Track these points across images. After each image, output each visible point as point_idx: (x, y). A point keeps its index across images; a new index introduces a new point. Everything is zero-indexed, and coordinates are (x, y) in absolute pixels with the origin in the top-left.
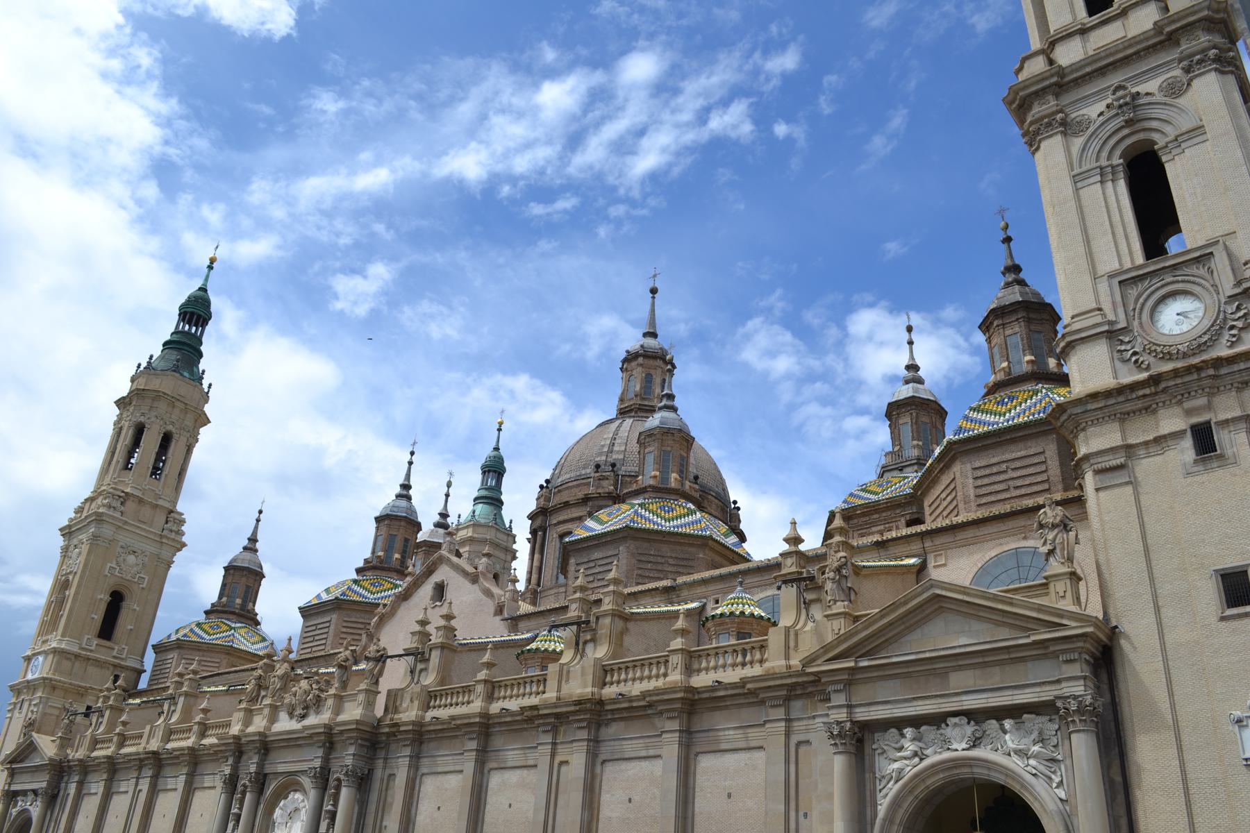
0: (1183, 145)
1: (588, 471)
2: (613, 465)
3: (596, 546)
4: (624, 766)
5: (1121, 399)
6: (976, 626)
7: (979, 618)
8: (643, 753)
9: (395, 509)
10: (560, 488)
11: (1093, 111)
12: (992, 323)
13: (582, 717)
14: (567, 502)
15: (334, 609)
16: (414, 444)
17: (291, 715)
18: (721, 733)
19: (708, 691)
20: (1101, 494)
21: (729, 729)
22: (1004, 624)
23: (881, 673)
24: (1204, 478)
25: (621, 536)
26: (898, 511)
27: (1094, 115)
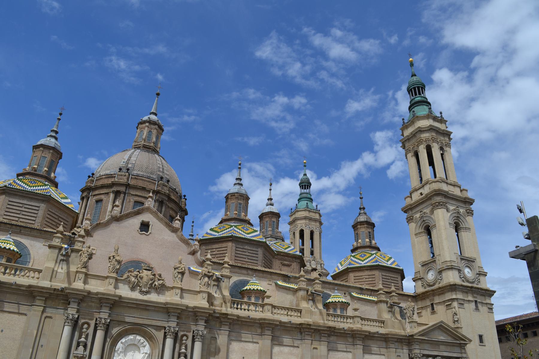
0: (467, 230)
1: (154, 177)
2: (168, 181)
3: (247, 243)
4: (336, 353)
5: (465, 288)
6: (445, 335)
7: (446, 333)
8: (345, 350)
9: (56, 146)
10: (137, 177)
11: (451, 208)
12: (364, 224)
13: (326, 332)
14: (145, 188)
15: (43, 201)
16: (63, 109)
17: (133, 289)
18: (372, 348)
19: (372, 334)
20: (460, 309)
21: (375, 347)
22: (450, 336)
23: (427, 342)
24: (476, 313)
25: (261, 244)
26: (294, 259)
27: (451, 209)
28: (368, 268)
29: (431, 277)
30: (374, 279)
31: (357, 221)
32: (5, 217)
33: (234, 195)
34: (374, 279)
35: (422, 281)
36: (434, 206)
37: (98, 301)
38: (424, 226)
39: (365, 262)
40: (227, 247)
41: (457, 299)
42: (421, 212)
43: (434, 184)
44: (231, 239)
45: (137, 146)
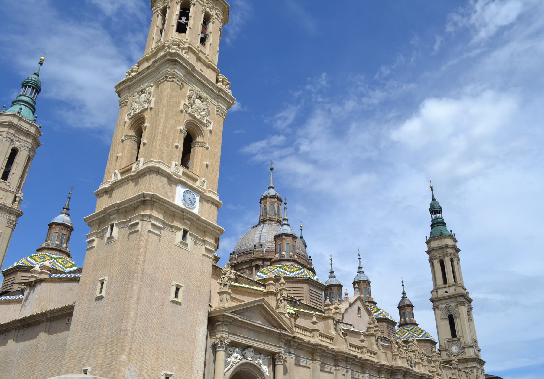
12: (410, 307)
14: (306, 266)
28: (424, 341)
29: (454, 350)
30: (427, 349)
31: (404, 303)
32: (311, 303)
33: (365, 282)
34: (427, 349)
35: (447, 352)
36: (459, 303)
37: (404, 374)
38: (448, 314)
39: (421, 336)
40: (383, 326)
41: (476, 367)
42: (447, 305)
43: (459, 288)
44: (386, 320)
45: (271, 219)
